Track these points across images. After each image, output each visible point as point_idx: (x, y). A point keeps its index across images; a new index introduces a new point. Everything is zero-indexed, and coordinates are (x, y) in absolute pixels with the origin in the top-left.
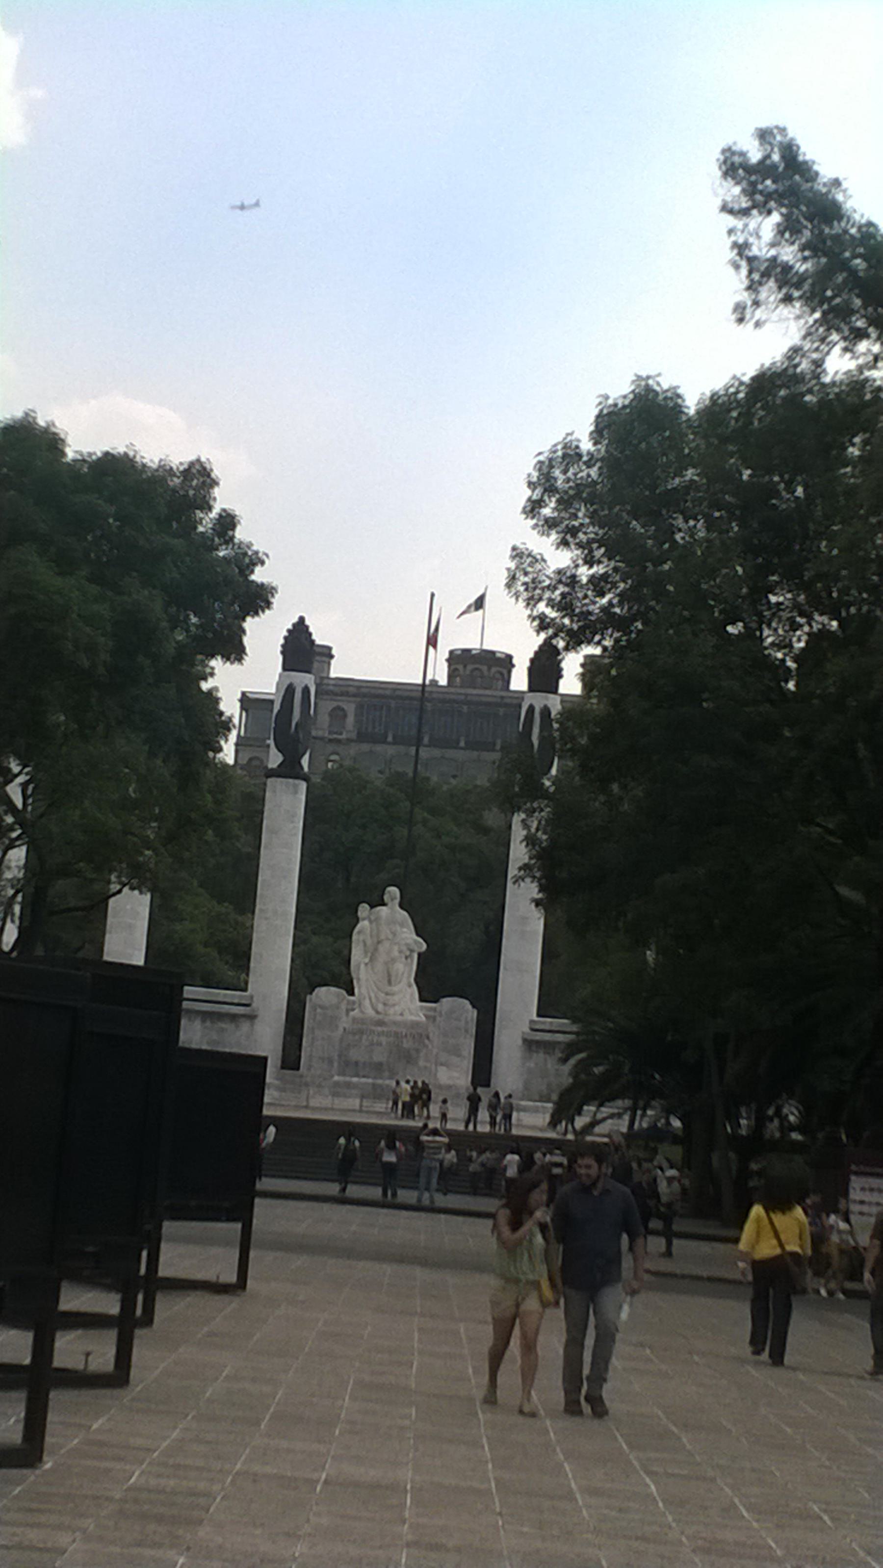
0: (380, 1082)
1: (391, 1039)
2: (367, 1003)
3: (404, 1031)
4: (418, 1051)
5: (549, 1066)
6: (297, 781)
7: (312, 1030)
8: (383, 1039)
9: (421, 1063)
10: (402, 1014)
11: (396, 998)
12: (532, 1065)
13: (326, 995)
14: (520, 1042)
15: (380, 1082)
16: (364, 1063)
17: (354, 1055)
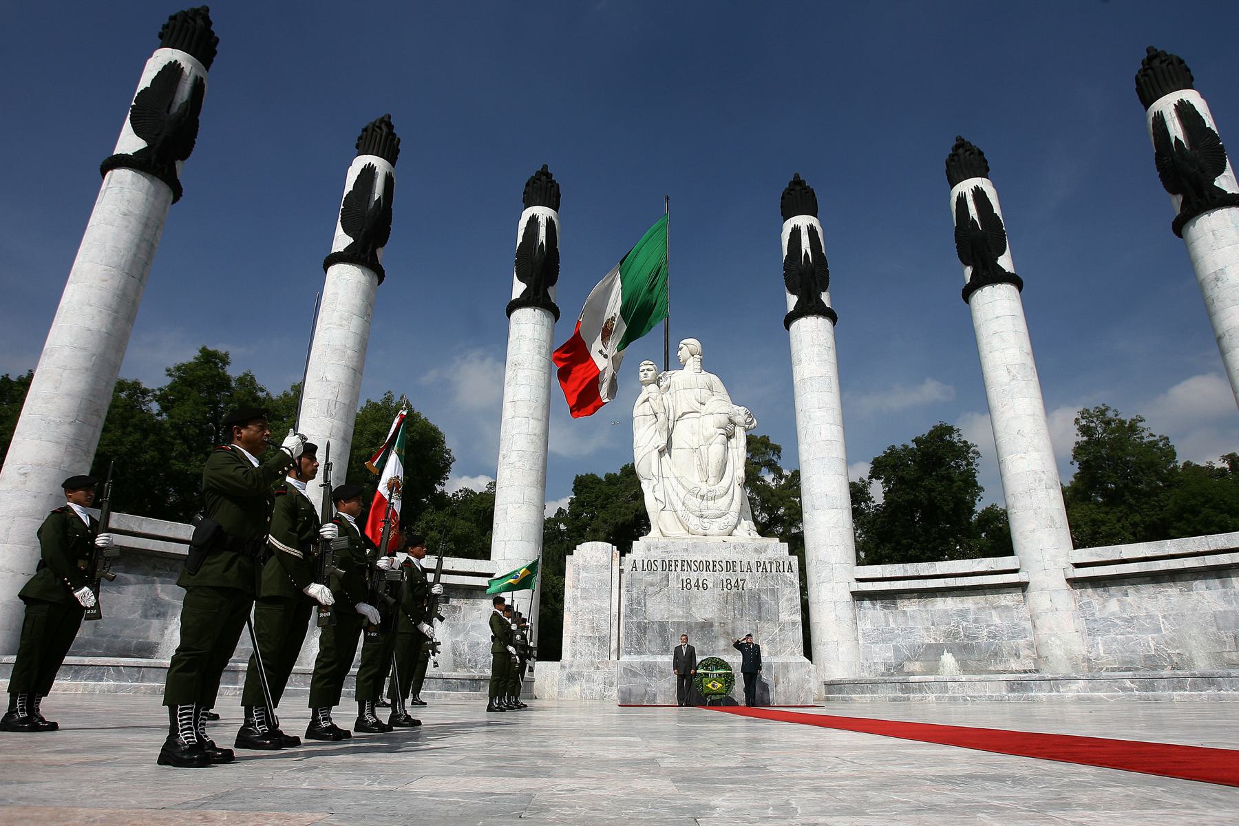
1: (724, 575)
2: (667, 516)
5: (892, 625)
7: (575, 598)
8: (709, 577)
12: (869, 626)
13: (590, 559)
14: (849, 597)
16: (679, 623)
17: (657, 610)
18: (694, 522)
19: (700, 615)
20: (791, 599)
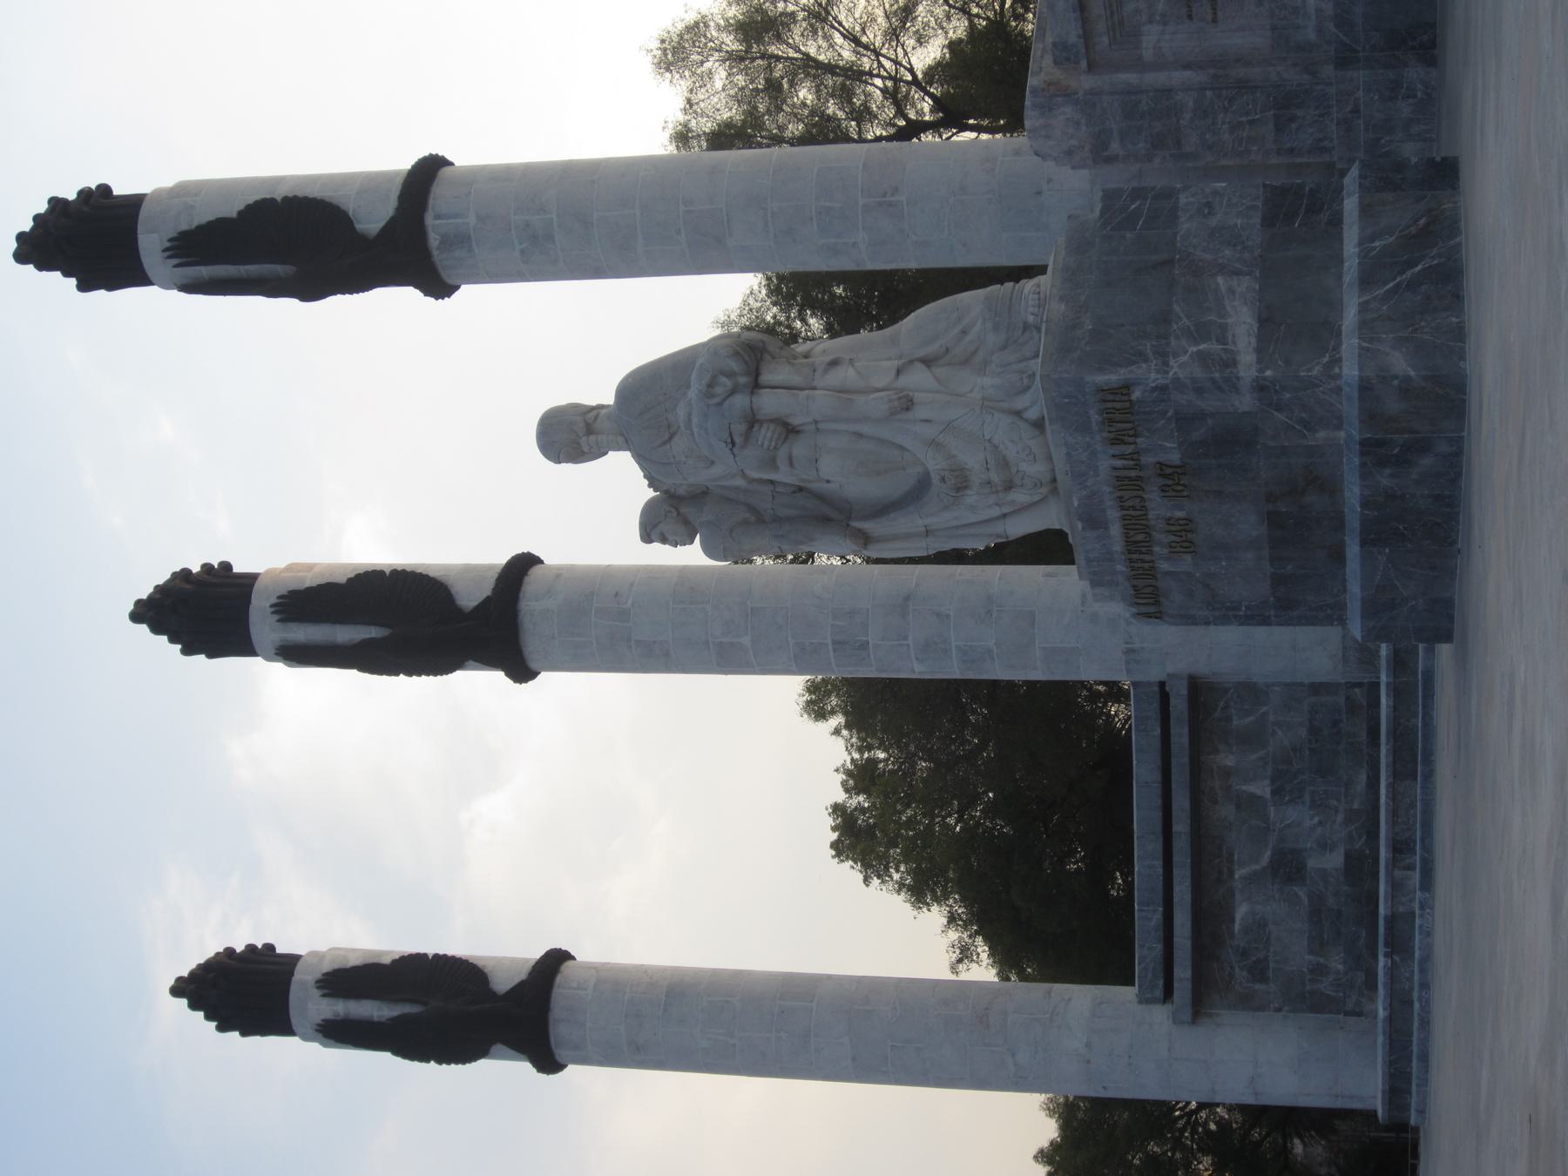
0: (1353, 520)
3: (1105, 464)
4: (1185, 420)
6: (434, 240)
9: (1245, 402)
10: (1039, 425)
11: (972, 460)
15: (1353, 520)
18: (1020, 497)
19: (1248, 524)
20: (1199, 391)
